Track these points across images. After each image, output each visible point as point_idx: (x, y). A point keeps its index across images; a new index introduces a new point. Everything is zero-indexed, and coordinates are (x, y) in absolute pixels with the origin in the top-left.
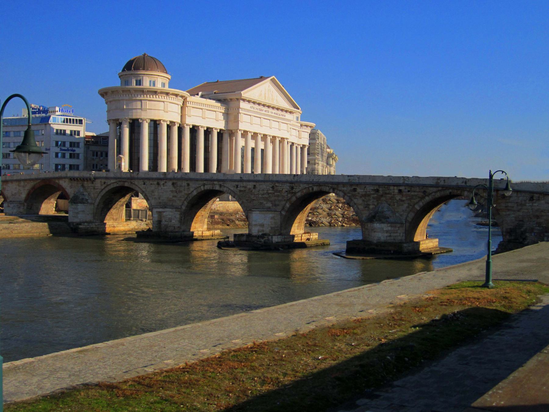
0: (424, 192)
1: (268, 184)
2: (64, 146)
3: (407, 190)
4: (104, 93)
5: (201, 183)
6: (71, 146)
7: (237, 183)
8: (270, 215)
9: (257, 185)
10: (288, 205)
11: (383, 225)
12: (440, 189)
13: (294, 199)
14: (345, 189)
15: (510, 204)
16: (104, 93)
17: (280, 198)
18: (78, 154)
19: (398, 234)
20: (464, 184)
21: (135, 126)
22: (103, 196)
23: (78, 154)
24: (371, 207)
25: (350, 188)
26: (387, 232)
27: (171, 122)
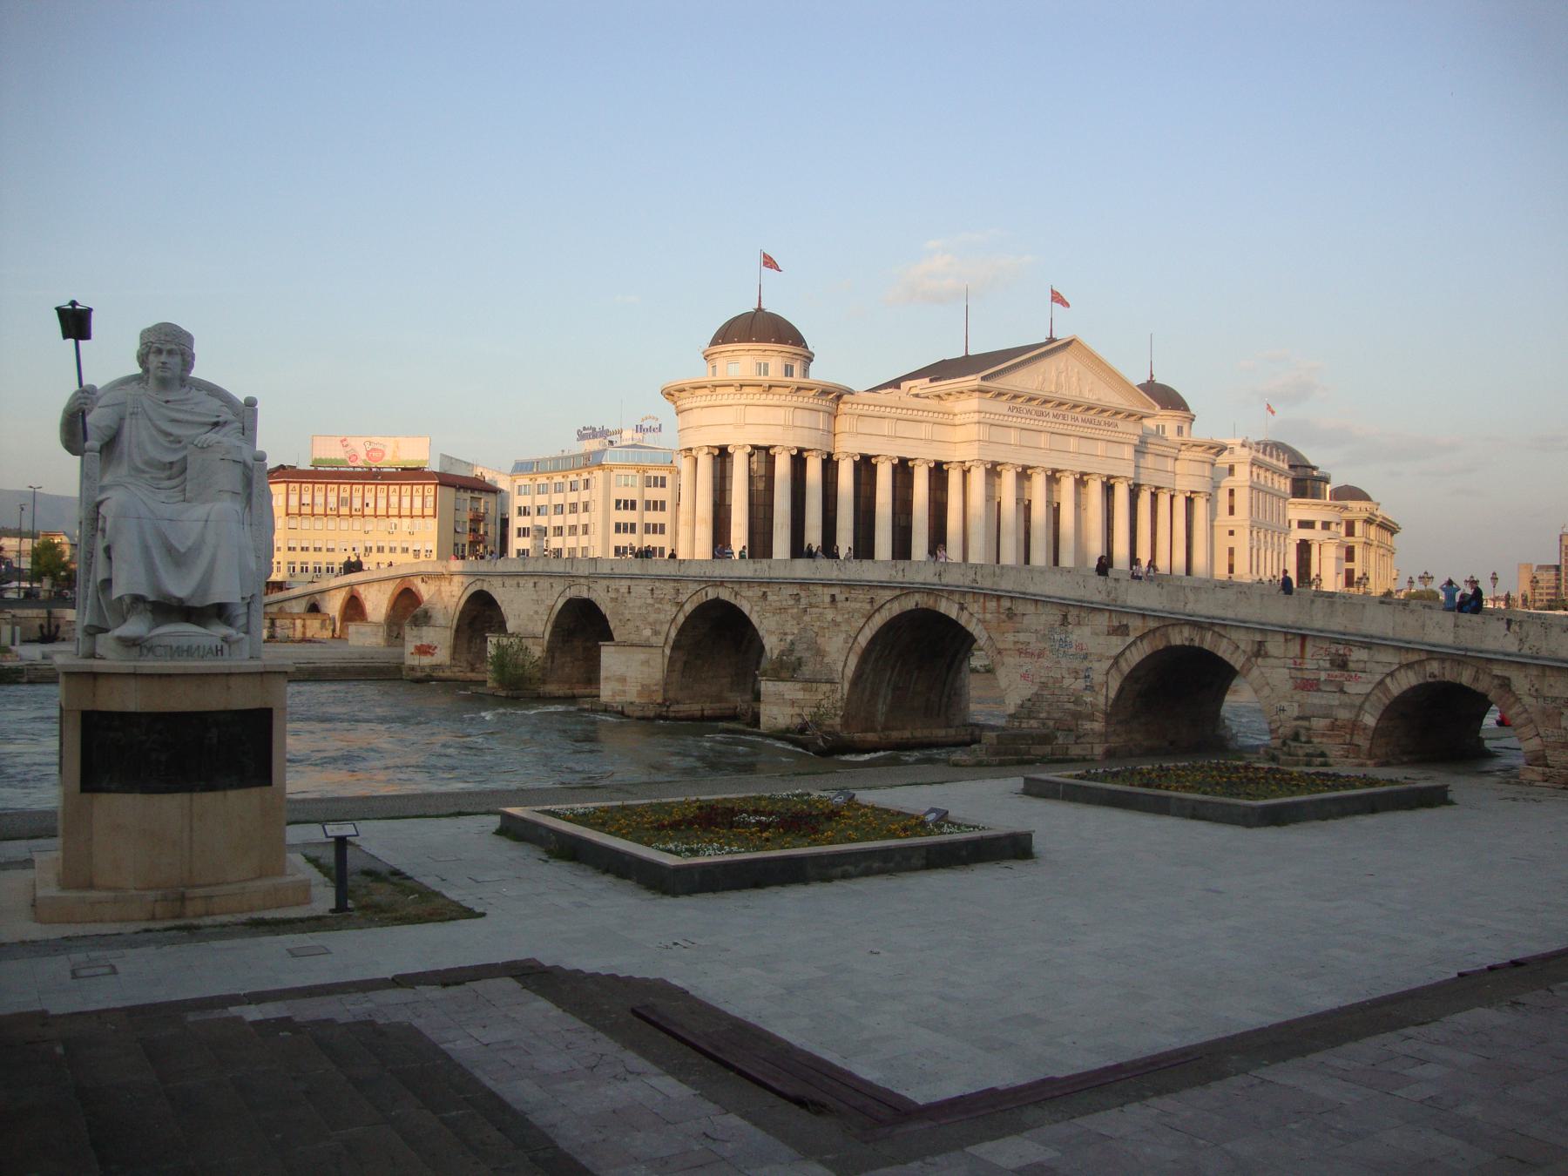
0: (872, 601)
1: (645, 583)
3: (843, 597)
7: (605, 582)
8: (640, 655)
9: (633, 583)
10: (673, 634)
12: (898, 592)
13: (681, 619)
14: (750, 593)
15: (1022, 637)
17: (662, 616)
20: (936, 580)
24: (789, 638)
25: (758, 591)
26: (793, 703)
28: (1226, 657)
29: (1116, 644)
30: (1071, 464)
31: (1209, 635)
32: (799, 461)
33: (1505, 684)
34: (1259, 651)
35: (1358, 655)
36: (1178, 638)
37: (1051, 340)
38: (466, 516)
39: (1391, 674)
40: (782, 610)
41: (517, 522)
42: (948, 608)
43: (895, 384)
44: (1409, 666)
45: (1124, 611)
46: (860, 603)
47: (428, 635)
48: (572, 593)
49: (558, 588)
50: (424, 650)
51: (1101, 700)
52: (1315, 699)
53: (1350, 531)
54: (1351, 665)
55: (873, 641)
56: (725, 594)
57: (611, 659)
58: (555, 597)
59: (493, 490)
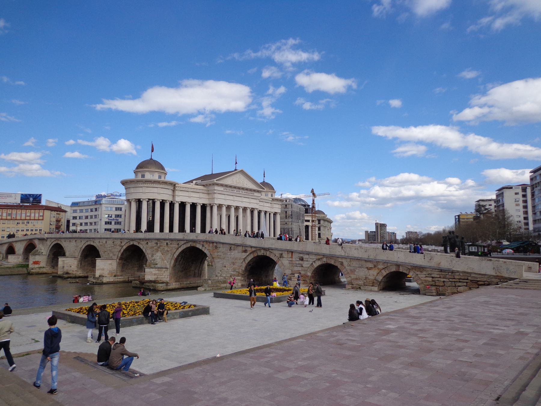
2: (111, 217)
4: (124, 183)
5: (86, 240)
6: (116, 217)
8: (109, 262)
10: (120, 255)
11: (152, 270)
13: (122, 251)
15: (219, 254)
16: (124, 183)
18: (121, 222)
19: (163, 276)
20: (195, 238)
21: (139, 202)
22: (50, 250)
23: (121, 222)
26: (155, 274)
27: (163, 200)
28: (273, 258)
29: (245, 255)
30: (242, 205)
31: (268, 252)
32: (163, 204)
33: (342, 264)
34: (281, 256)
35: (305, 257)
36: (261, 253)
37: (236, 170)
38: (54, 219)
39: (314, 262)
40: (152, 247)
41: (72, 221)
42: (199, 246)
43: (191, 181)
44: (319, 259)
45: (246, 246)
46: (175, 245)
47: (37, 258)
48: (88, 243)
49: (83, 242)
50: (36, 263)
51: (241, 270)
52: (296, 269)
53: (319, 223)
54: (304, 259)
55: (178, 256)
56: (136, 243)
57: (99, 263)
58: (82, 245)
59: (65, 212)
